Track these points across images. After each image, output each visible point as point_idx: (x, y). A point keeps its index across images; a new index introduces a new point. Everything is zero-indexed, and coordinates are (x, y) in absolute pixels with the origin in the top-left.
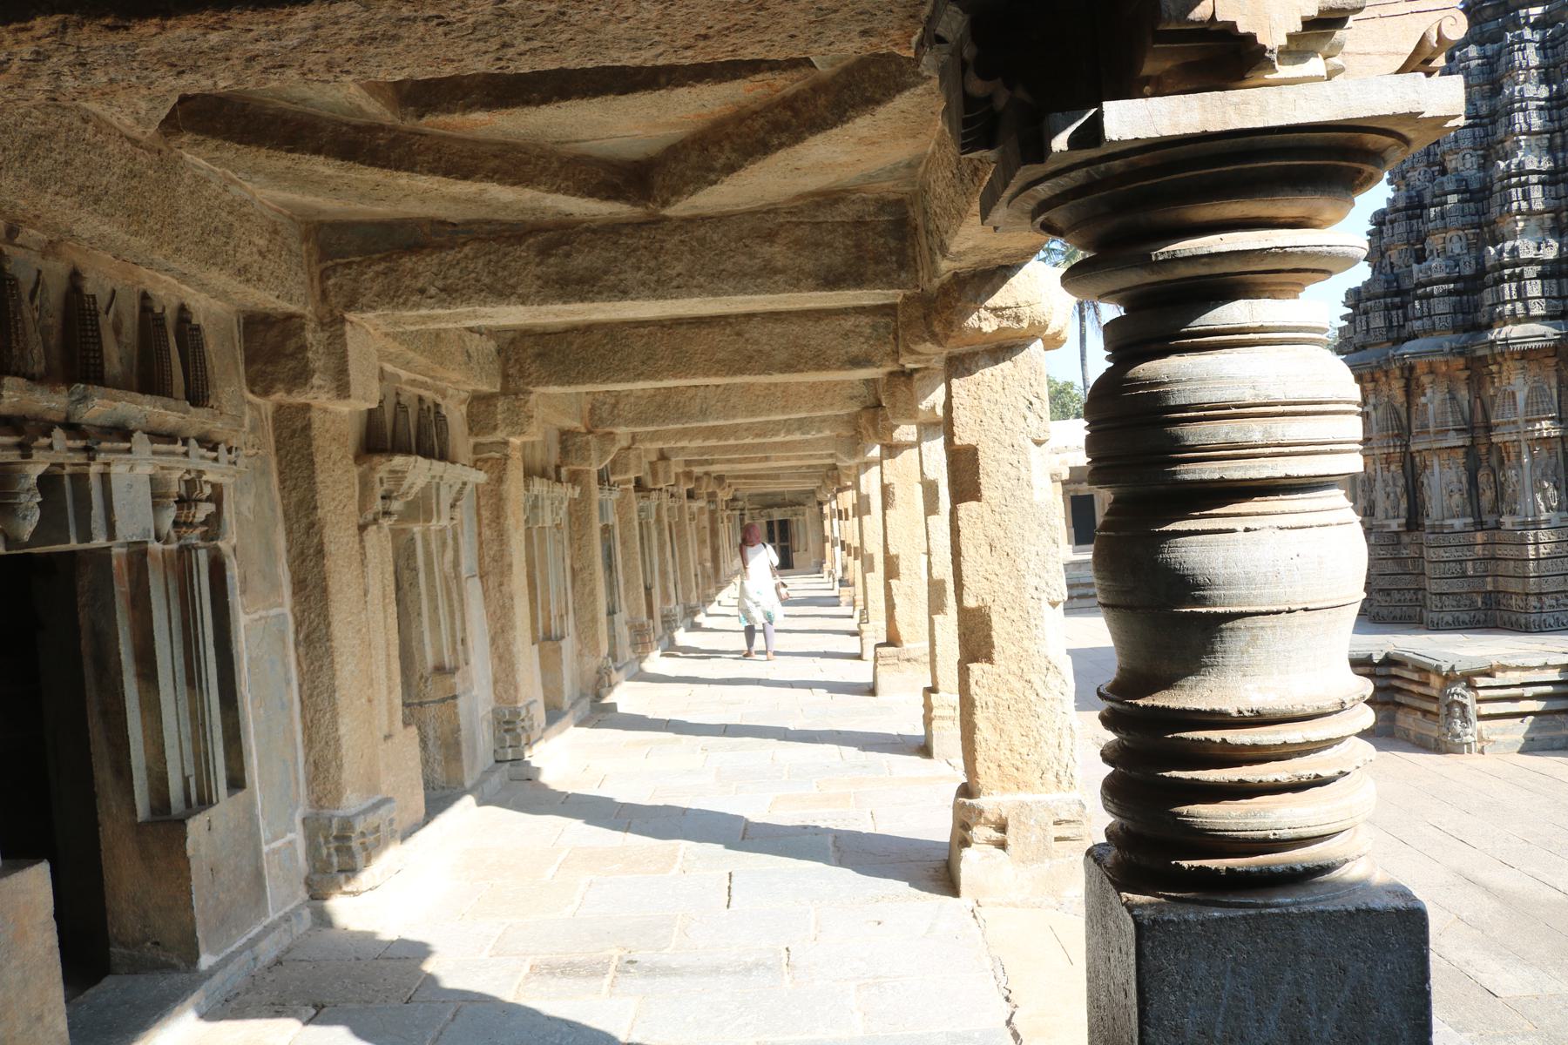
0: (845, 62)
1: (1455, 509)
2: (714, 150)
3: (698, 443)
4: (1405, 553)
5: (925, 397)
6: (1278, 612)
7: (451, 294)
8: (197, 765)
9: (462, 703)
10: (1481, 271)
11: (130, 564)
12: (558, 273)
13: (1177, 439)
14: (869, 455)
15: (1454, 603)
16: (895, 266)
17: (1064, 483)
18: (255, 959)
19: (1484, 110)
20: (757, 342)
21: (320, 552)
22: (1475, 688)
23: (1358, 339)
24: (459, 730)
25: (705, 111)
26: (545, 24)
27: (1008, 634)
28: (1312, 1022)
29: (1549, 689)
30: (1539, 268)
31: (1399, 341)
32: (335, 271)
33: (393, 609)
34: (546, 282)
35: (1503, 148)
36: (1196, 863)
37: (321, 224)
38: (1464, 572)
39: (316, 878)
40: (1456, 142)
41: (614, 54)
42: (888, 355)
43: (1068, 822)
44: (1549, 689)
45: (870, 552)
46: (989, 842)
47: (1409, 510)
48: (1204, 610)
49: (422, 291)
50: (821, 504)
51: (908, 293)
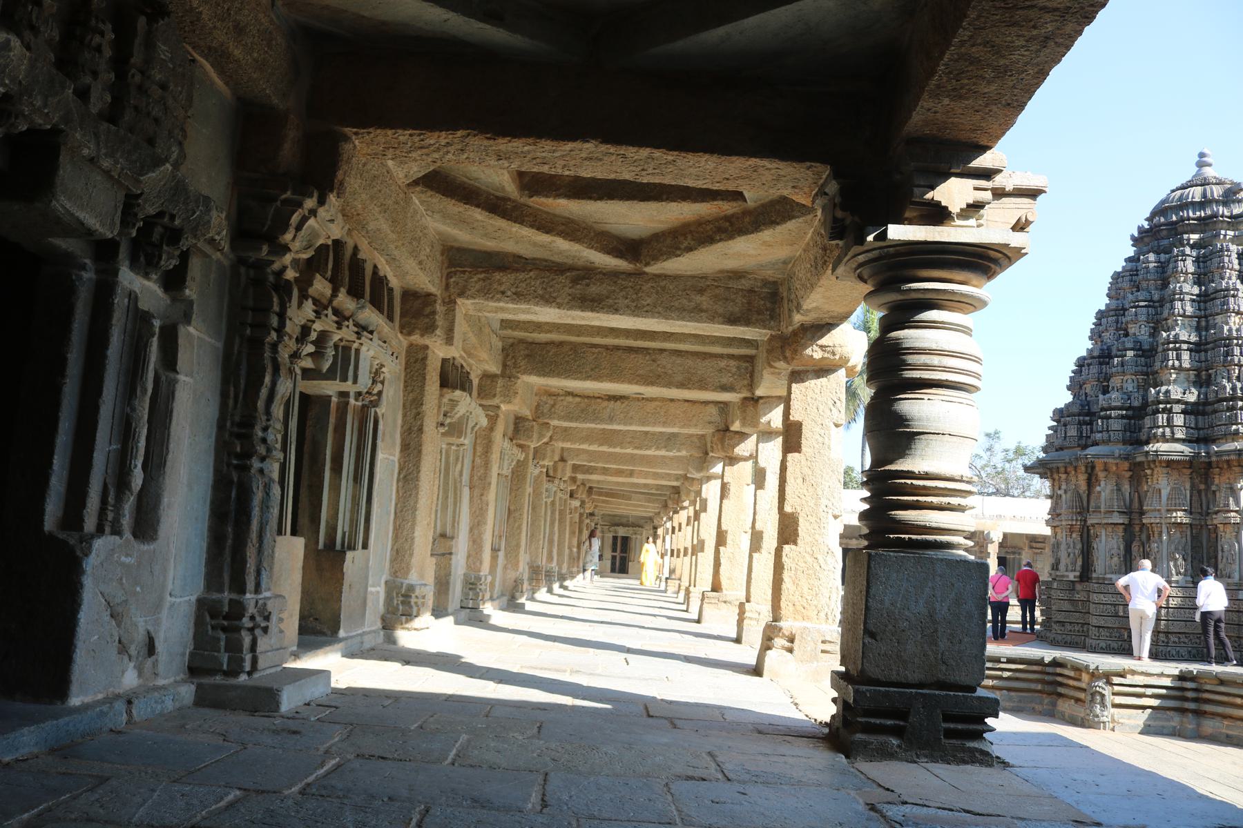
0: (762, 202)
1: (1114, 567)
2: (681, 238)
4: (1077, 597)
5: (765, 415)
6: (938, 434)
7: (519, 296)
8: (351, 526)
10: (1145, 404)
12: (581, 294)
13: (904, 361)
14: (711, 471)
15: (1108, 634)
18: (362, 643)
19: (1156, 297)
20: (664, 367)
21: (421, 430)
22: (1112, 684)
23: (1058, 443)
24: (450, 575)
25: (682, 217)
26: (665, 164)
28: (937, 605)
29: (1164, 691)
30: (1183, 406)
31: (1085, 447)
32: (455, 274)
35: (1167, 324)
37: (452, 247)
38: (1117, 613)
39: (389, 616)
40: (1136, 315)
41: (686, 180)
43: (830, 642)
44: (1164, 691)
45: (702, 538)
46: (783, 648)
47: (1083, 566)
49: (503, 293)
50: (655, 528)
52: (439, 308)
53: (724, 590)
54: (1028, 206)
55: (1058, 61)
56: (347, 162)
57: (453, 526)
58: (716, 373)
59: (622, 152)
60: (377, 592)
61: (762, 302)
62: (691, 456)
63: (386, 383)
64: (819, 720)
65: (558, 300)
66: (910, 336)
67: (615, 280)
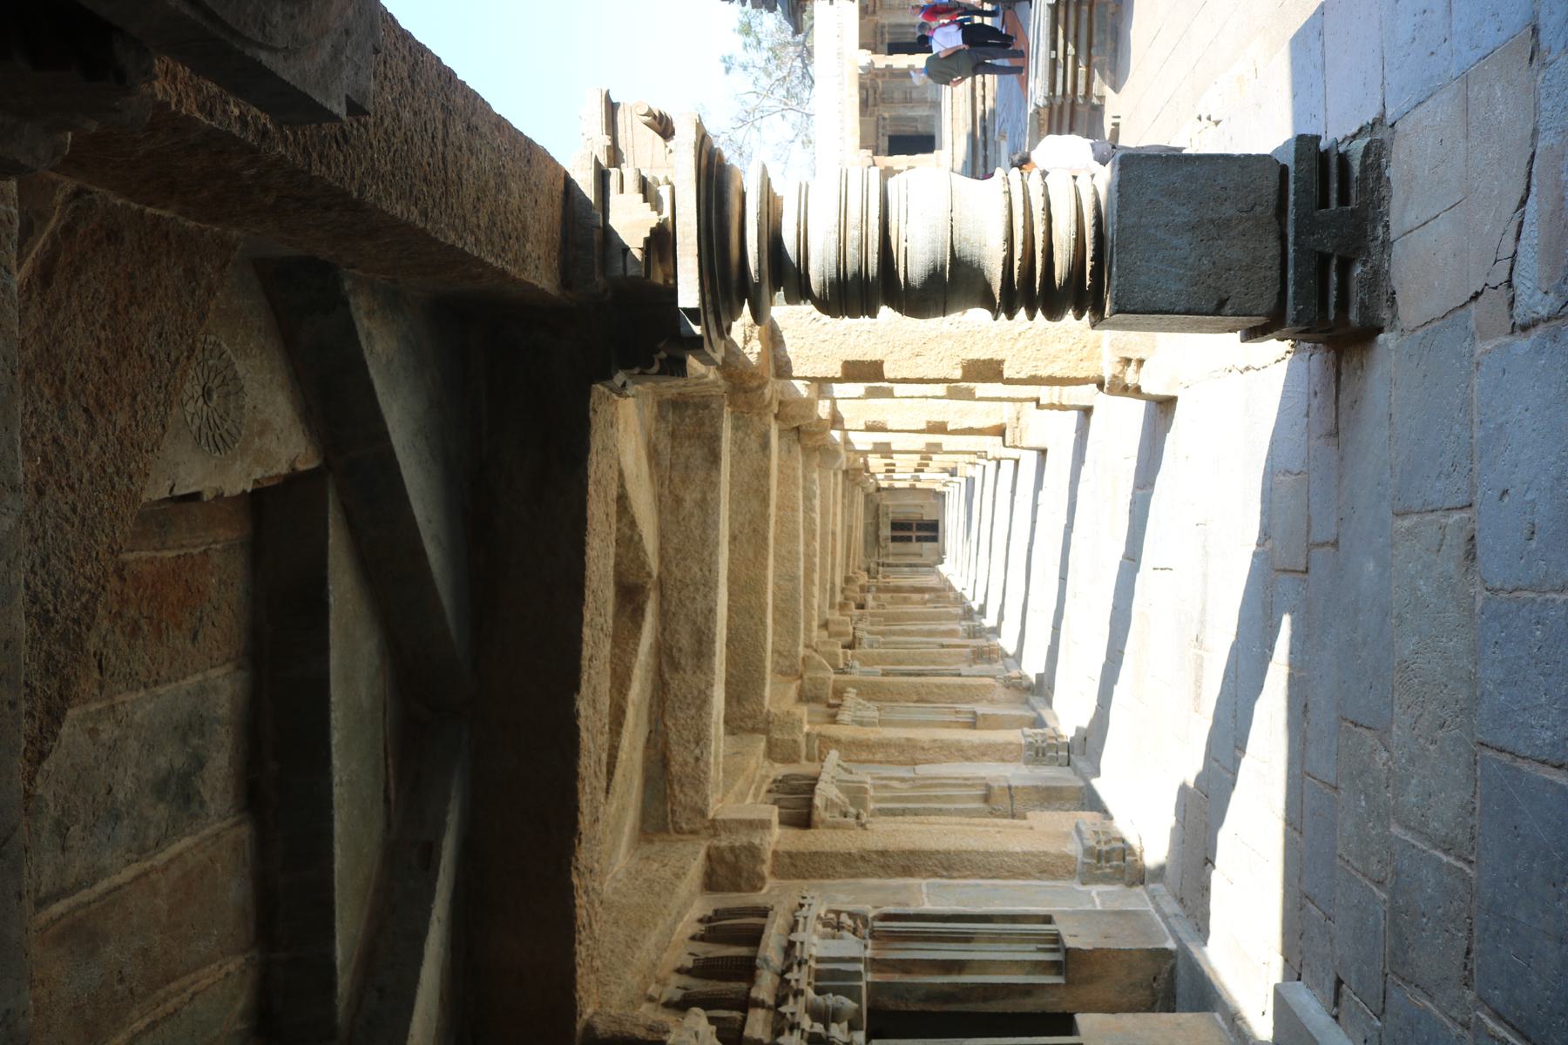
3: (816, 590)
6: (952, 226)
7: (701, 739)
8: (1029, 941)
9: (1014, 783)
11: (879, 971)
13: (854, 275)
16: (706, 411)
18: (1176, 915)
20: (742, 525)
21: (883, 853)
28: (1179, 220)
32: (677, 823)
33: (932, 818)
34: (699, 667)
36: (1088, 277)
39: (1127, 878)
42: (761, 419)
46: (1137, 372)
48: (948, 266)
49: (697, 759)
50: (879, 489)
51: (726, 403)
52: (724, 842)
53: (1003, 421)
54: (628, 112)
55: (488, 104)
56: (620, 1024)
57: (972, 786)
58: (746, 456)
59: (587, 663)
60: (1099, 896)
62: (819, 466)
63: (835, 907)
65: (703, 687)
66: (819, 269)
67: (670, 614)
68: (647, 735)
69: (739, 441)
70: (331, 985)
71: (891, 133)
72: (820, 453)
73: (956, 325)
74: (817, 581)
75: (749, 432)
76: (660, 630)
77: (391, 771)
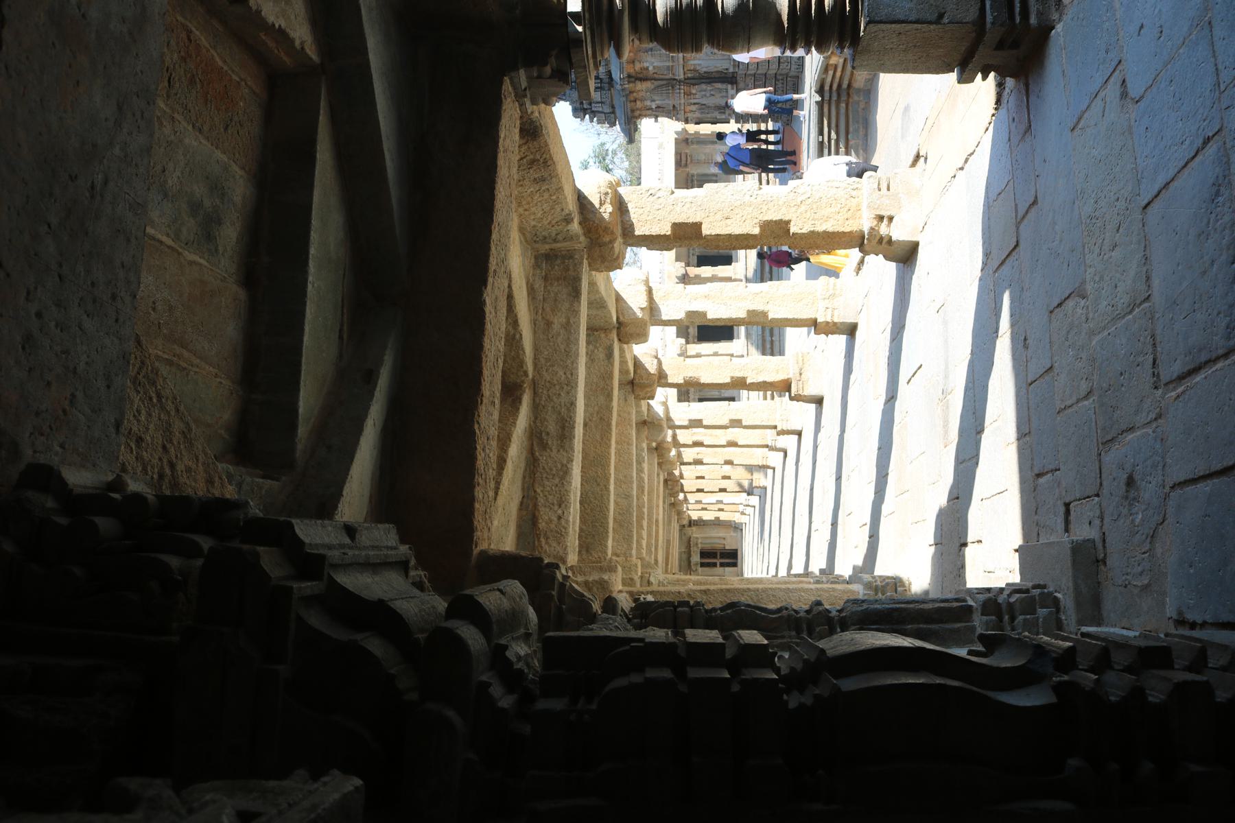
5: (635, 313)
13: (687, 5)
14: (662, 416)
16: (571, 261)
17: (687, 342)
20: (592, 415)
23: (607, 110)
27: (775, 212)
34: (562, 446)
36: (848, 4)
42: (607, 336)
43: (879, 184)
45: (728, 422)
47: (723, 82)
49: (560, 518)
50: (692, 523)
51: (585, 256)
58: (595, 364)
61: (556, 267)
62: (647, 439)
64: (994, 111)
65: (565, 462)
67: (541, 406)
68: (520, 500)
69: (590, 353)
70: (293, 426)
71: (699, 254)
72: (648, 428)
73: (754, 196)
74: (645, 528)
75: (598, 345)
76: (533, 419)
77: (345, 320)
